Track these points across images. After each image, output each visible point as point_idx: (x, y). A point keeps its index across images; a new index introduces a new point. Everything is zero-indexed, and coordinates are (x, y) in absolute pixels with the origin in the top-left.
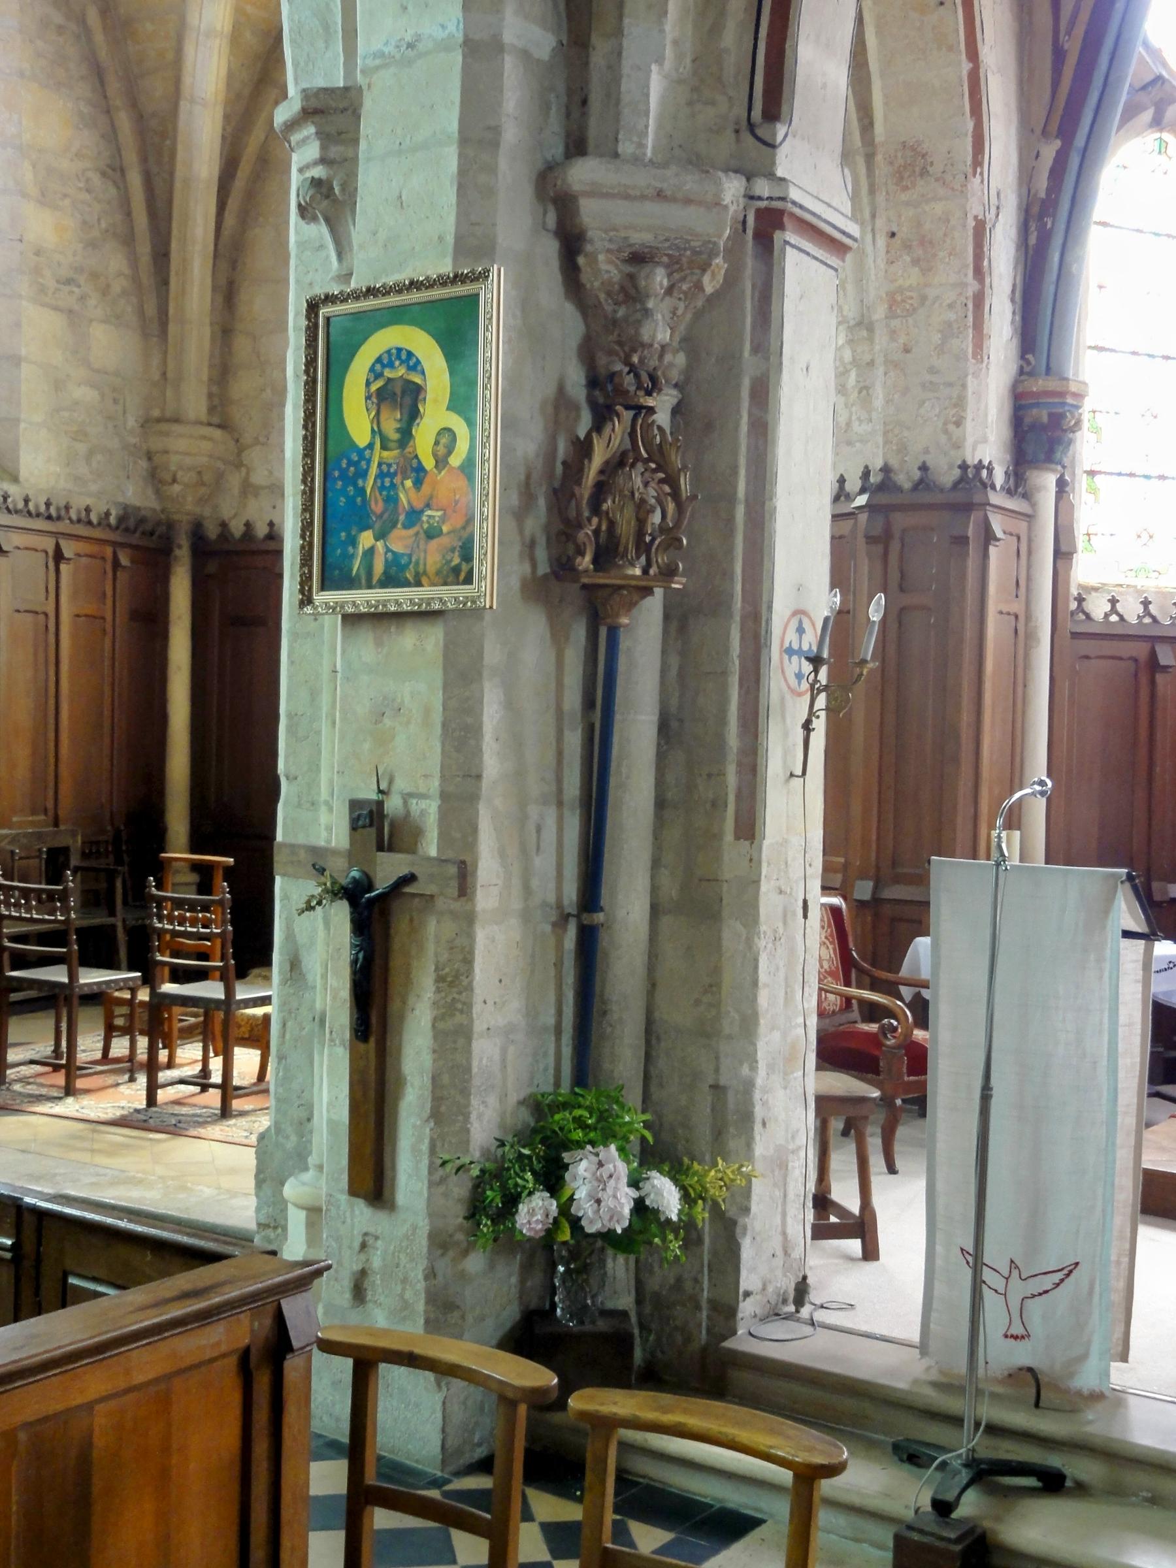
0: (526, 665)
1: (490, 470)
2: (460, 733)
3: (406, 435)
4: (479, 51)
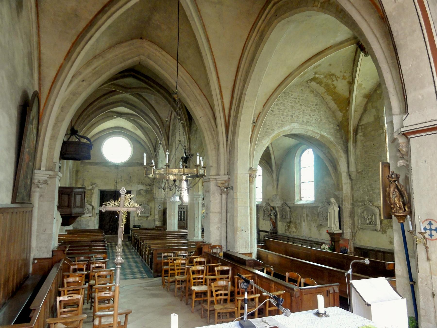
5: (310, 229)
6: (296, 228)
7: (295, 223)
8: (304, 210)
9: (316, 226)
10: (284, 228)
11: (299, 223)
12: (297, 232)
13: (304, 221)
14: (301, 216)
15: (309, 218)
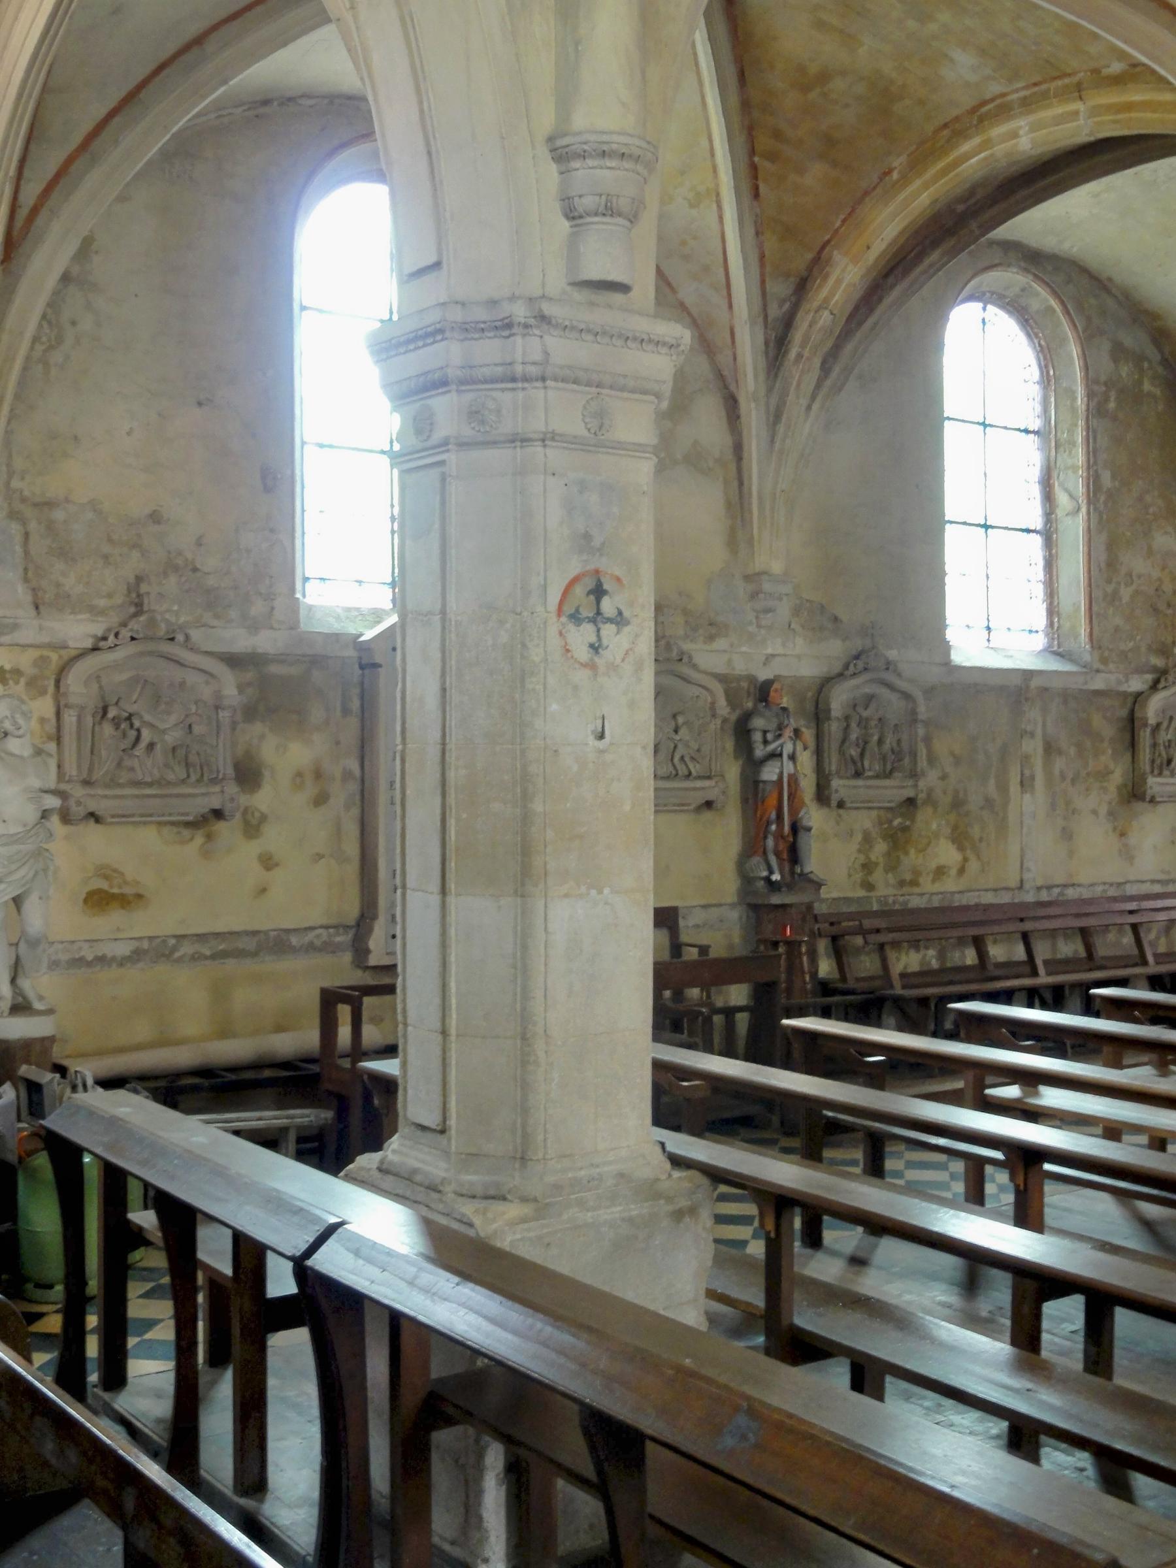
5: (1067, 835)
6: (960, 838)
7: (958, 804)
8: (1033, 714)
9: (1103, 810)
11: (989, 803)
12: (973, 866)
13: (1026, 784)
14: (1004, 753)
15: (1059, 764)
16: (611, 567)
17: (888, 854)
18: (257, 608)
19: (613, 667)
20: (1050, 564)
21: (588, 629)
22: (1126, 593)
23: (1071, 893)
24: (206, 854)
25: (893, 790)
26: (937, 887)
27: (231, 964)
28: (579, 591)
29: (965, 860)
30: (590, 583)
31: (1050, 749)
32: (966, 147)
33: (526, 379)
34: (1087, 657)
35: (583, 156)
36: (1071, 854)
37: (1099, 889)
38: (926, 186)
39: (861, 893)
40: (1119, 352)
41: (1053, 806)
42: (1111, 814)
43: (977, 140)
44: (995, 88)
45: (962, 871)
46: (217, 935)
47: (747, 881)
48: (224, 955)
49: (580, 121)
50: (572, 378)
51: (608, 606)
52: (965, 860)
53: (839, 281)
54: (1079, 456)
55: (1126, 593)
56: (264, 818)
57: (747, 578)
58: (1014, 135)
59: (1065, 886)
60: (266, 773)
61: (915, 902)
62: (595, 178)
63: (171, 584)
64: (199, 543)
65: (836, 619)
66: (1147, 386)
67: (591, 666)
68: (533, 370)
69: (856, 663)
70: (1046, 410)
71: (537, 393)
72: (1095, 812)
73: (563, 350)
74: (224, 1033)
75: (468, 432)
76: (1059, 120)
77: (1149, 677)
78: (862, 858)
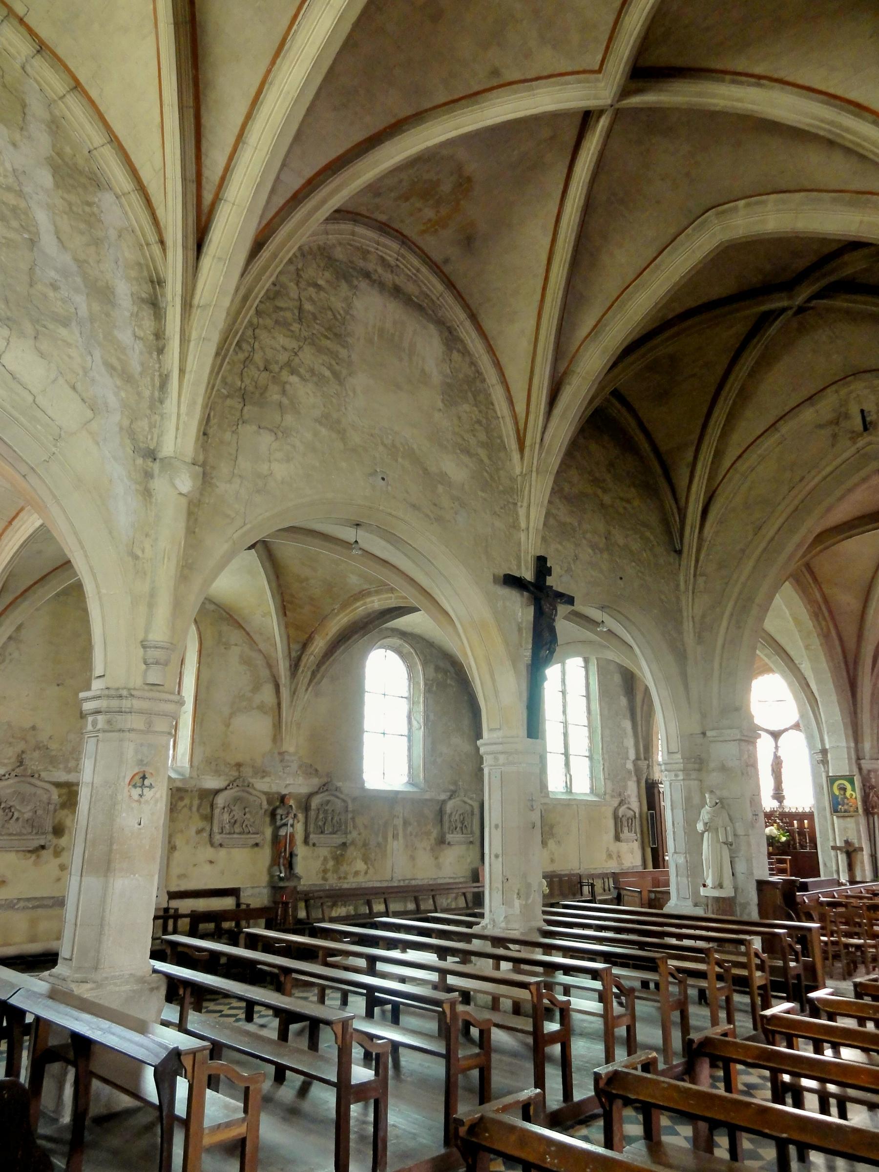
0: (862, 821)
1: (859, 797)
2: (859, 831)
3: (845, 794)
4: (848, 748)
5: (412, 858)
6: (366, 859)
7: (365, 845)
9: (429, 848)
10: (317, 865)
11: (379, 845)
12: (371, 871)
15: (410, 829)
16: (149, 770)
17: (334, 865)
18: (72, 764)
19: (147, 802)
20: (410, 749)
21: (139, 791)
22: (439, 760)
23: (413, 883)
24: (36, 864)
25: (338, 839)
26: (355, 880)
27: (39, 911)
28: (137, 778)
29: (368, 868)
30: (141, 775)
31: (406, 823)
32: (358, 604)
33: (125, 712)
34: (422, 785)
35: (150, 647)
36: (414, 866)
37: (407, 882)
38: (346, 615)
39: (322, 882)
40: (437, 669)
41: (407, 846)
42: (432, 849)
43: (362, 602)
44: (366, 587)
45: (366, 873)
46: (35, 898)
47: (271, 876)
48: (38, 907)
49: (151, 637)
50: (141, 712)
51: (147, 782)
52: (368, 868)
53: (317, 645)
54: (421, 707)
55: (439, 760)
56: (63, 849)
57: (280, 754)
58: (373, 602)
59: (411, 880)
60: (67, 831)
61: (345, 886)
62: (153, 654)
63: (36, 754)
64: (50, 738)
65: (316, 770)
66: (449, 681)
67: (139, 801)
68: (128, 710)
69: (324, 787)
70: (409, 690)
71: (129, 716)
72: (425, 849)
73: (137, 704)
74: (33, 939)
75: (106, 727)
76: (386, 599)
77: (449, 794)
78: (323, 867)
